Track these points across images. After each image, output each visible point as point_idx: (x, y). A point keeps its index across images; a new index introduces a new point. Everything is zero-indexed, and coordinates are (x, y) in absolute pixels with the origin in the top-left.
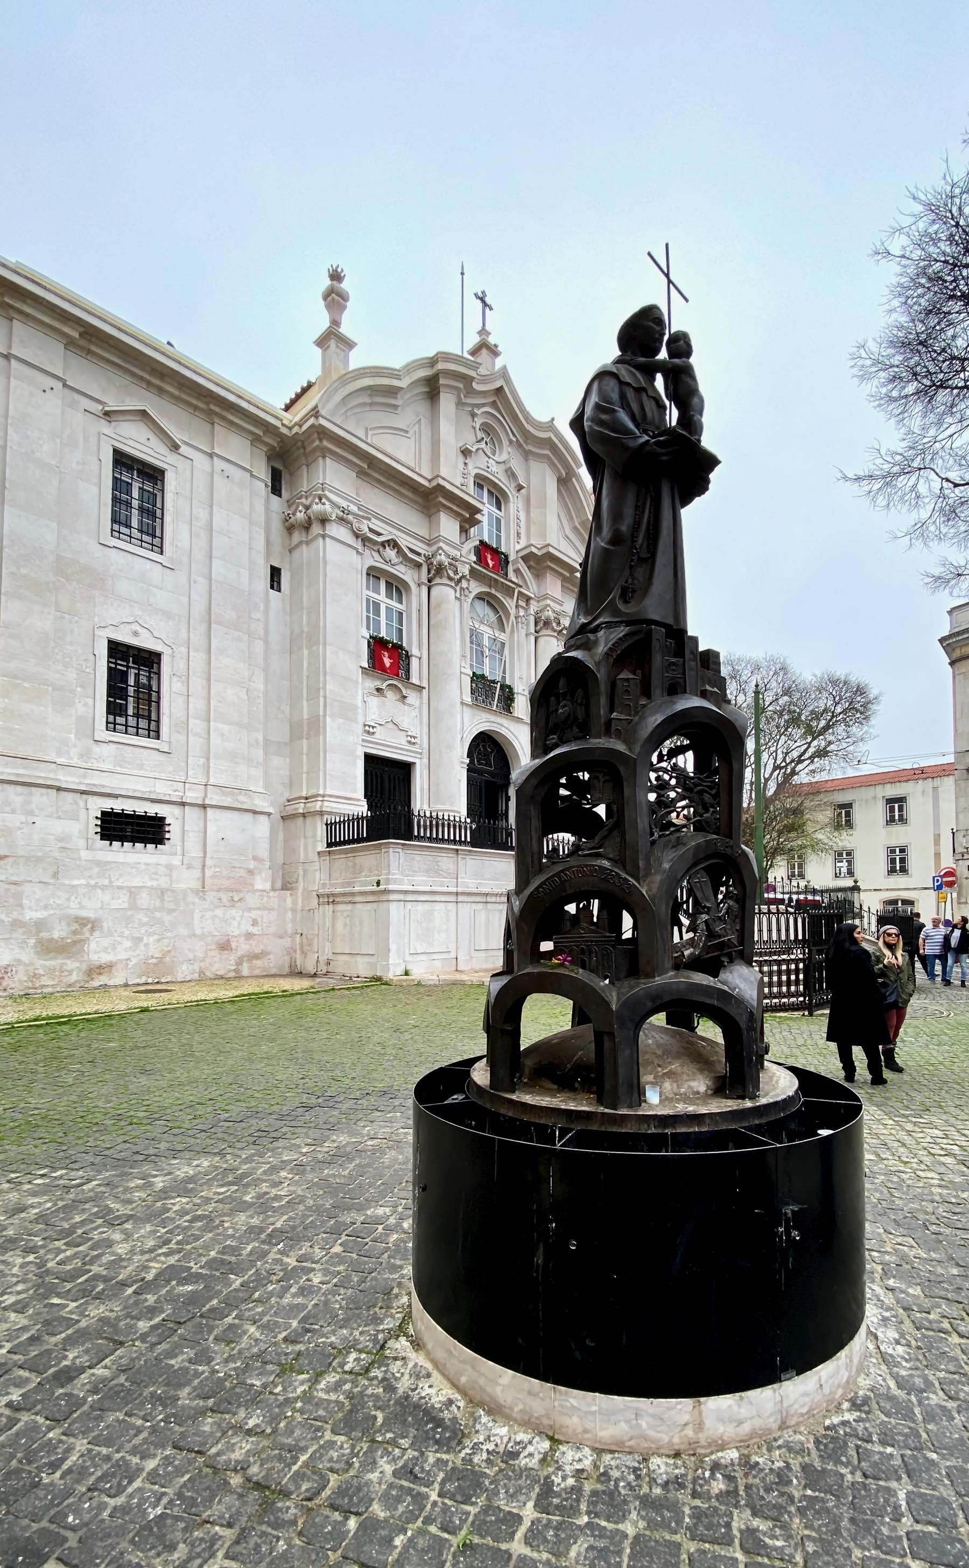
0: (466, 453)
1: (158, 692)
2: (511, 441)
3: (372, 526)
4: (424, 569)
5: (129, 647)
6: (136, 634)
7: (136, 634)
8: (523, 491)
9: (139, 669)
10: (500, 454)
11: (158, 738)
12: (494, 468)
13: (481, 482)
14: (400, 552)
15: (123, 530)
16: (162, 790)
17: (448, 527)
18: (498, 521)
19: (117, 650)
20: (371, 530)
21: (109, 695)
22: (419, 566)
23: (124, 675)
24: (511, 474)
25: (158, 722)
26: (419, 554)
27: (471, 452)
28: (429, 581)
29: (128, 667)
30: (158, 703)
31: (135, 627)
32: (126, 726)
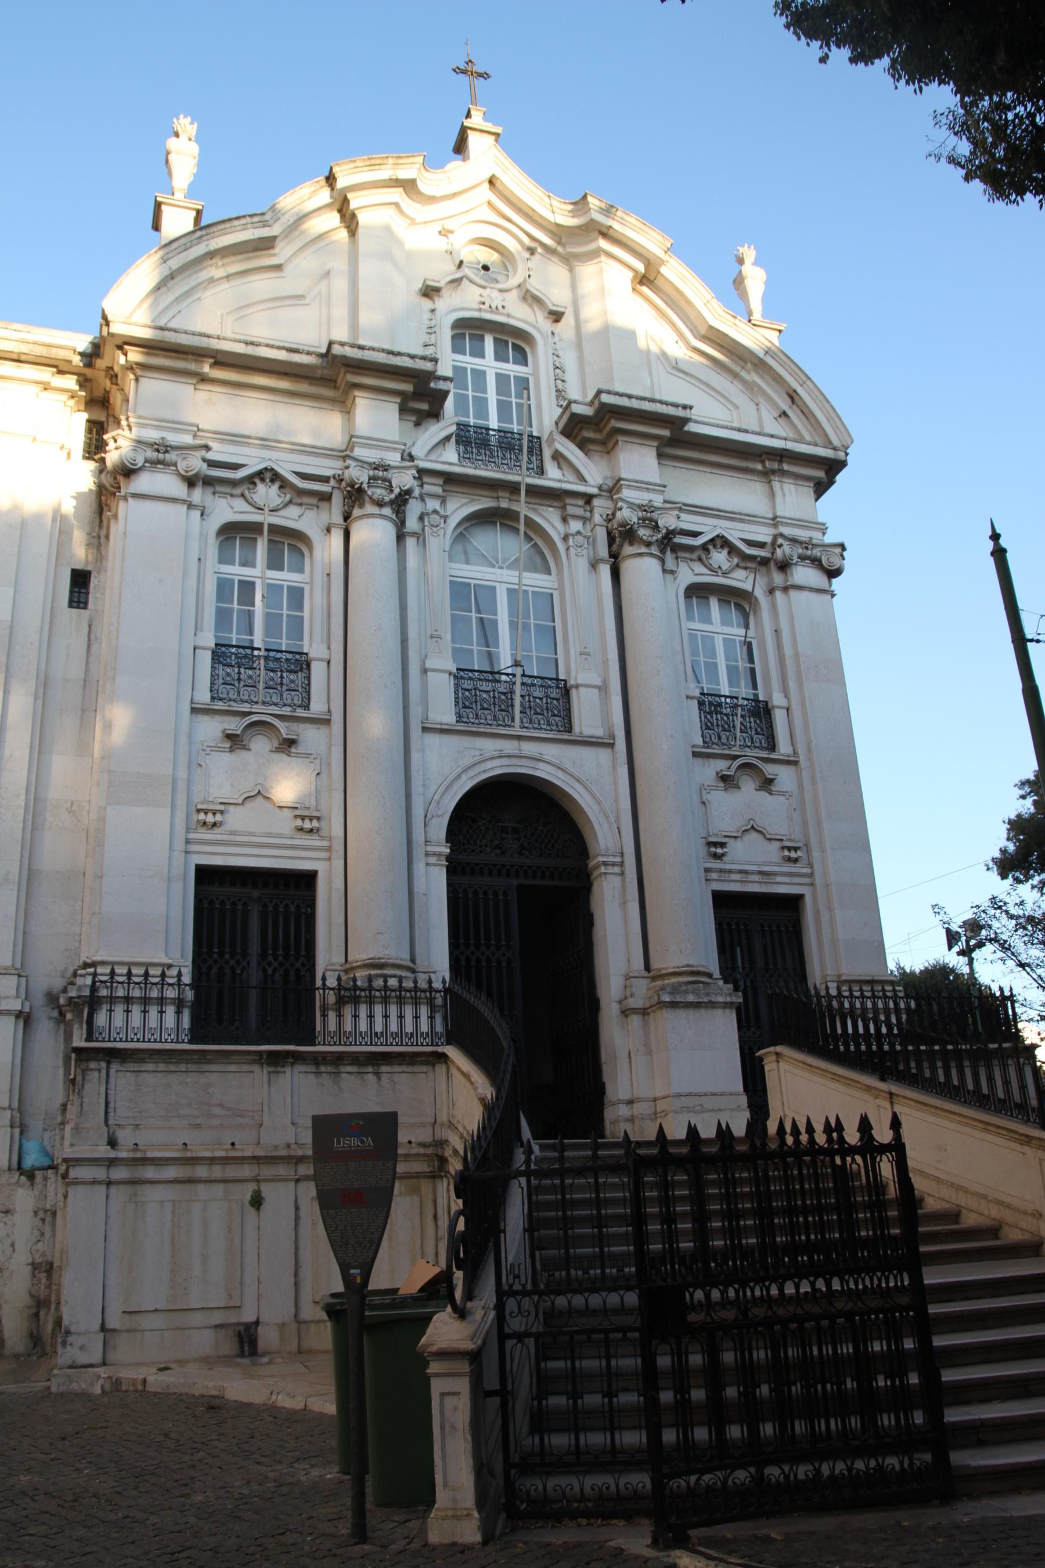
0: (429, 292)
2: (532, 251)
3: (210, 456)
4: (337, 499)
8: (568, 319)
10: (515, 274)
12: (494, 298)
13: (470, 330)
14: (285, 486)
17: (375, 417)
18: (523, 384)
20: (212, 464)
22: (326, 497)
24: (531, 298)
26: (325, 480)
27: (437, 290)
28: (346, 518)
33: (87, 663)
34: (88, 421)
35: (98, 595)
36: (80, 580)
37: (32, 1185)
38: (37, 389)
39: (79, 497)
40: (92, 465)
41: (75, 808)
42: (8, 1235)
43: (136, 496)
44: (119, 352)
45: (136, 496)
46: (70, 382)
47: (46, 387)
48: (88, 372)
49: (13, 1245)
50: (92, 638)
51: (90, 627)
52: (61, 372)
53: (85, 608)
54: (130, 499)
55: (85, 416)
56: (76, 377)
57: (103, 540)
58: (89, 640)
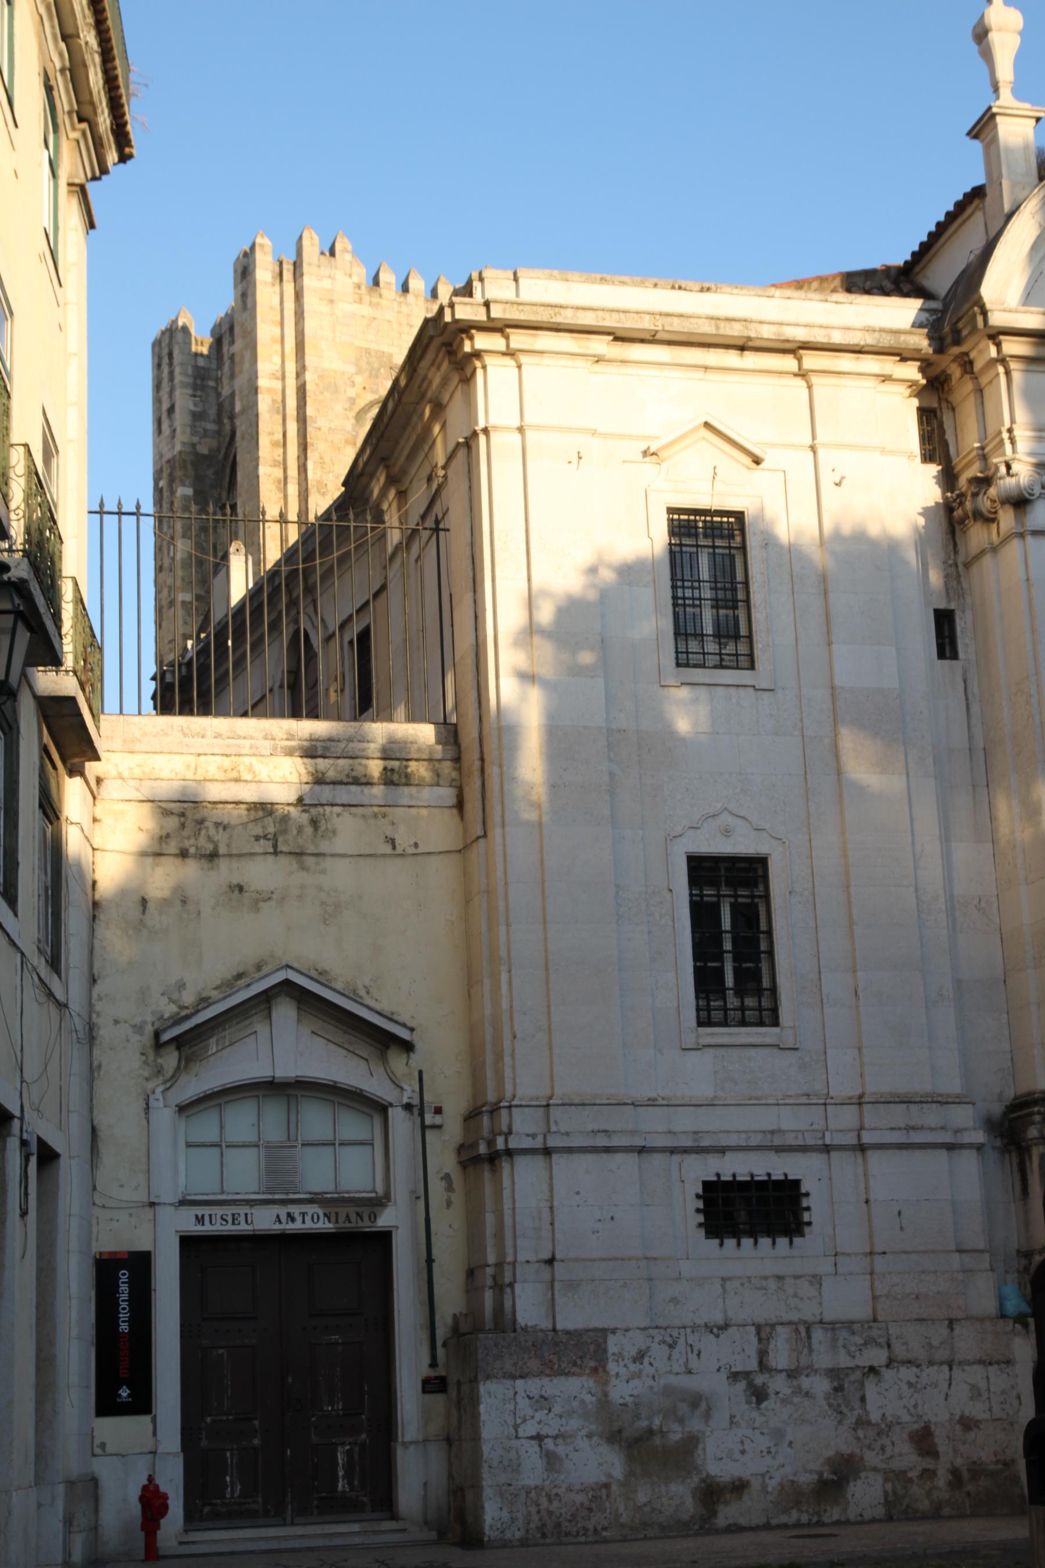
1: (769, 933)
5: (716, 860)
6: (727, 833)
7: (727, 833)
9: (736, 896)
11: (776, 1023)
15: (694, 646)
16: (794, 1122)
19: (703, 870)
21: (697, 956)
23: (715, 908)
25: (774, 990)
29: (718, 896)
30: (771, 953)
31: (726, 819)
32: (725, 1010)
33: (969, 727)
34: (919, 409)
35: (967, 641)
36: (944, 623)
37: (1028, 1333)
38: (871, 383)
39: (926, 512)
40: (934, 469)
41: (983, 904)
42: (1012, 1387)
43: (1035, 533)
44: (990, 343)
45: (1035, 533)
46: (911, 371)
47: (886, 378)
48: (936, 358)
49: (1019, 1397)
50: (970, 696)
51: (965, 682)
52: (904, 359)
53: (955, 656)
54: (1029, 539)
55: (915, 402)
56: (918, 364)
57: (961, 568)
58: (967, 699)
